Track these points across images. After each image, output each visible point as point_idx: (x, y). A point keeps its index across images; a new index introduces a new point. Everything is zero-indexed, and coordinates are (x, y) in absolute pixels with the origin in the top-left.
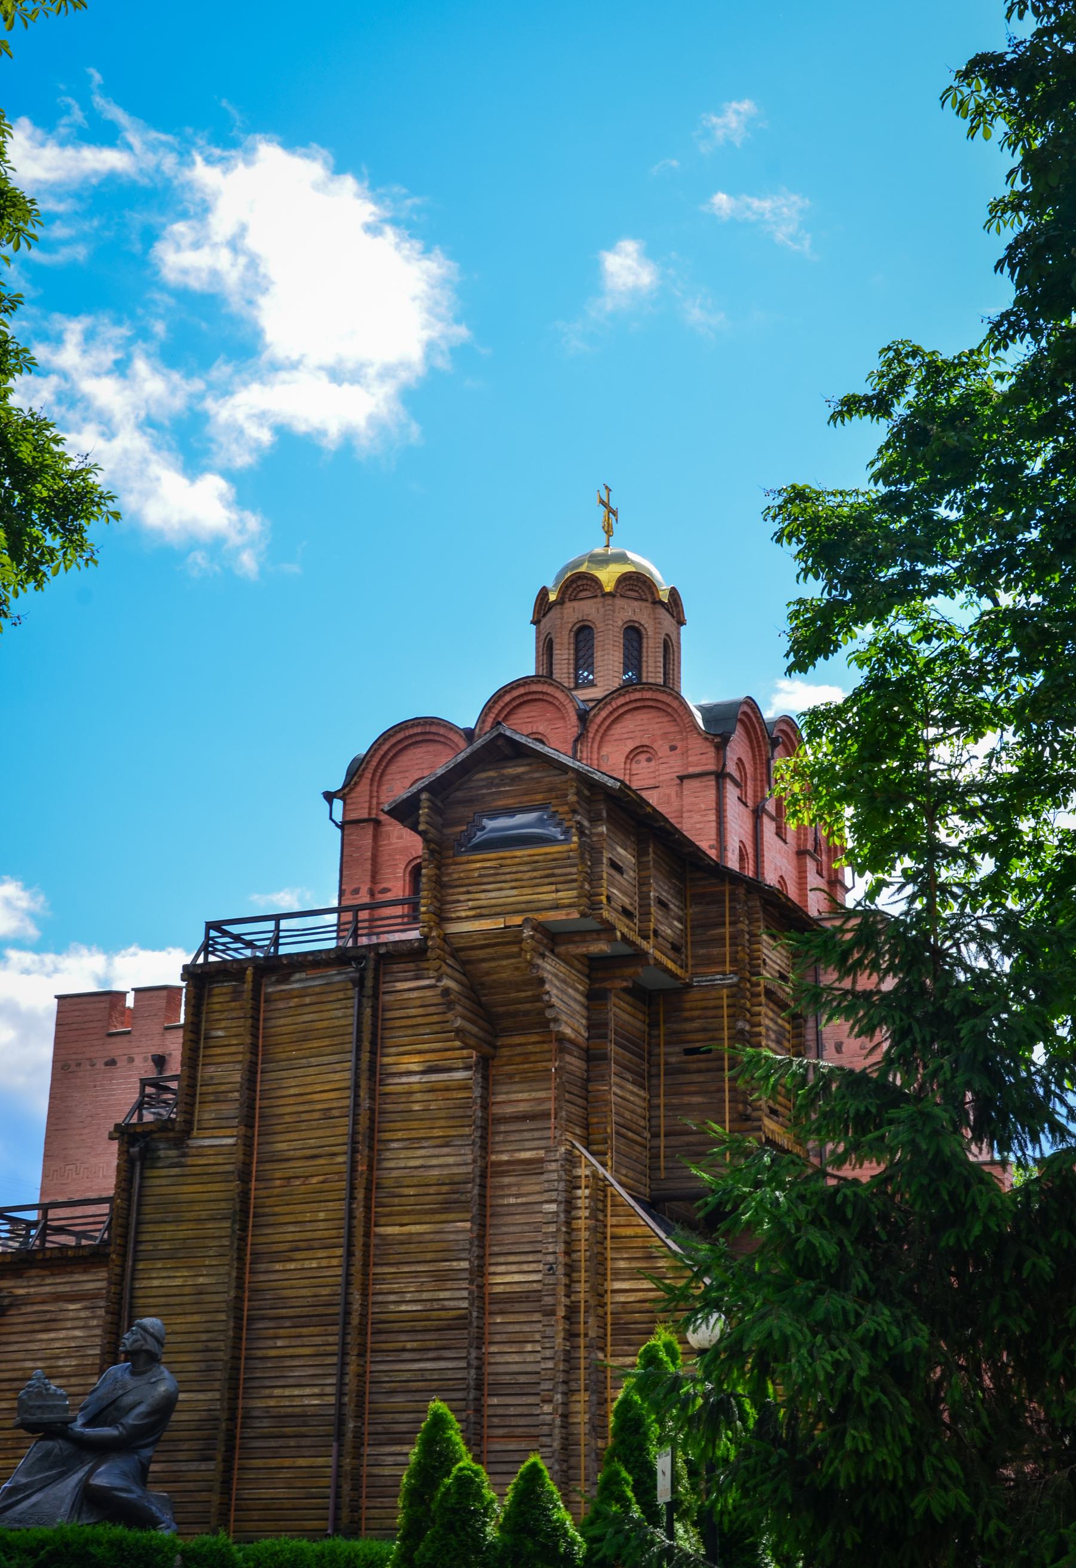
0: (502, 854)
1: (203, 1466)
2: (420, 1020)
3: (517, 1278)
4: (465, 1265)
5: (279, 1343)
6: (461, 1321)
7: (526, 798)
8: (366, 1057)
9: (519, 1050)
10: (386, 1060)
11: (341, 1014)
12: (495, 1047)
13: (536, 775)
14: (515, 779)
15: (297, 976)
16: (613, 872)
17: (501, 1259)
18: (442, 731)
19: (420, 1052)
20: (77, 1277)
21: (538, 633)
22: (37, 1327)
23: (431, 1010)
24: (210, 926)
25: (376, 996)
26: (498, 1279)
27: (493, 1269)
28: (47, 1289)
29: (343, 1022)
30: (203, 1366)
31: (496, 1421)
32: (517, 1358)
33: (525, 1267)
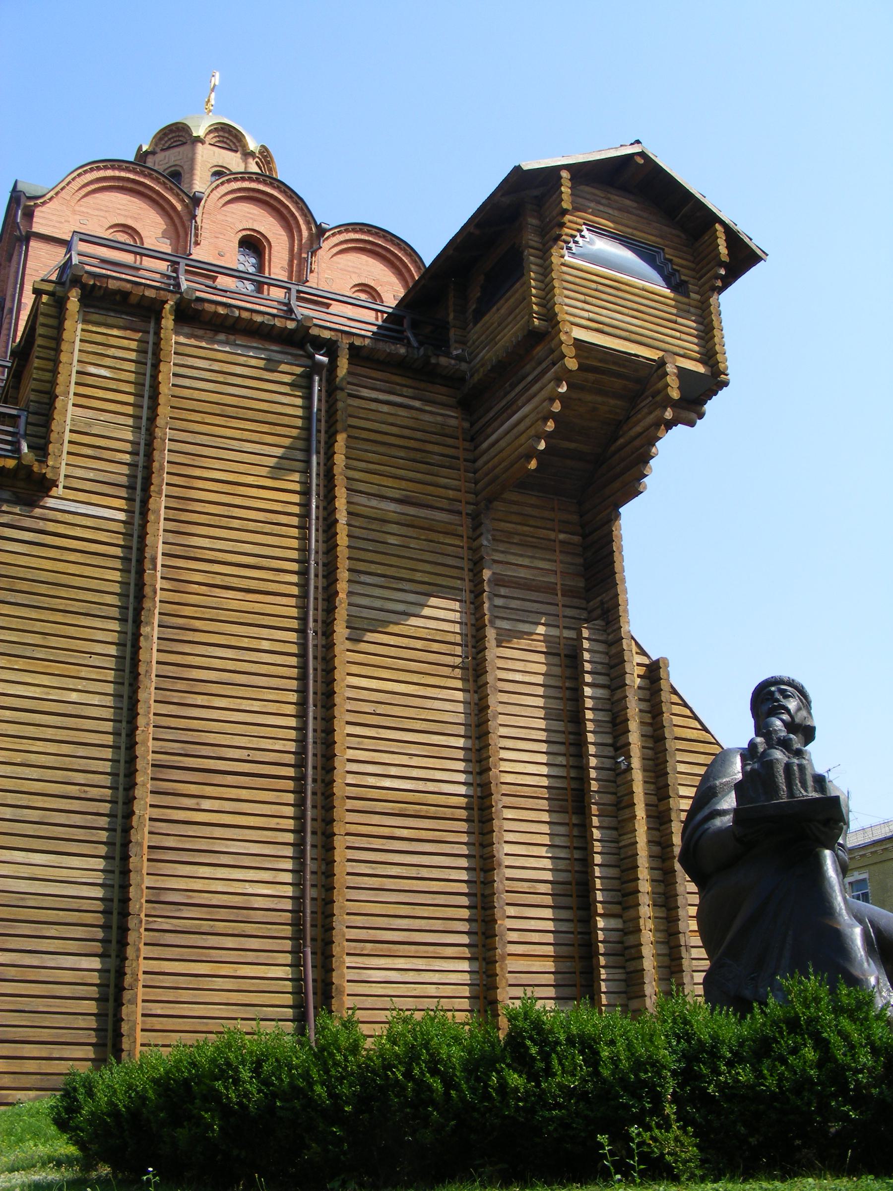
5: (206, 804)
9: (515, 508)
23: (406, 432)
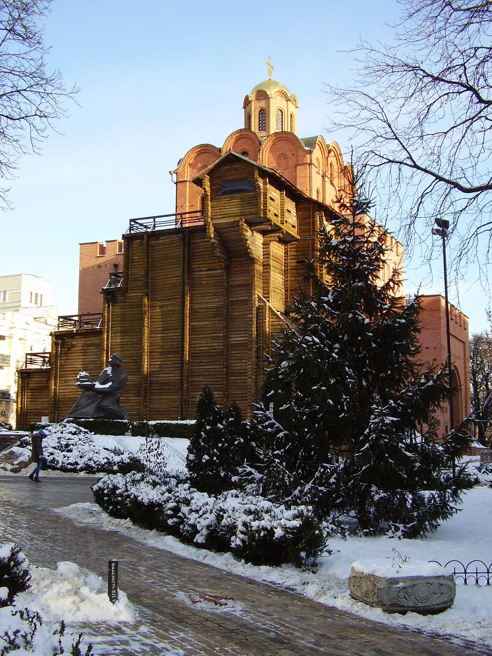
0: (232, 196)
1: (137, 398)
2: (205, 253)
3: (239, 339)
4: (222, 334)
6: (221, 353)
7: (239, 176)
8: (186, 265)
10: (194, 266)
11: (178, 251)
12: (231, 262)
13: (243, 168)
14: (236, 169)
15: (162, 238)
16: (271, 201)
17: (234, 333)
18: (211, 149)
19: (205, 264)
20: (92, 339)
21: (245, 111)
23: (209, 249)
24: (131, 220)
25: (189, 245)
27: (231, 336)
29: (178, 254)
31: (233, 384)
32: (240, 365)
33: (242, 335)
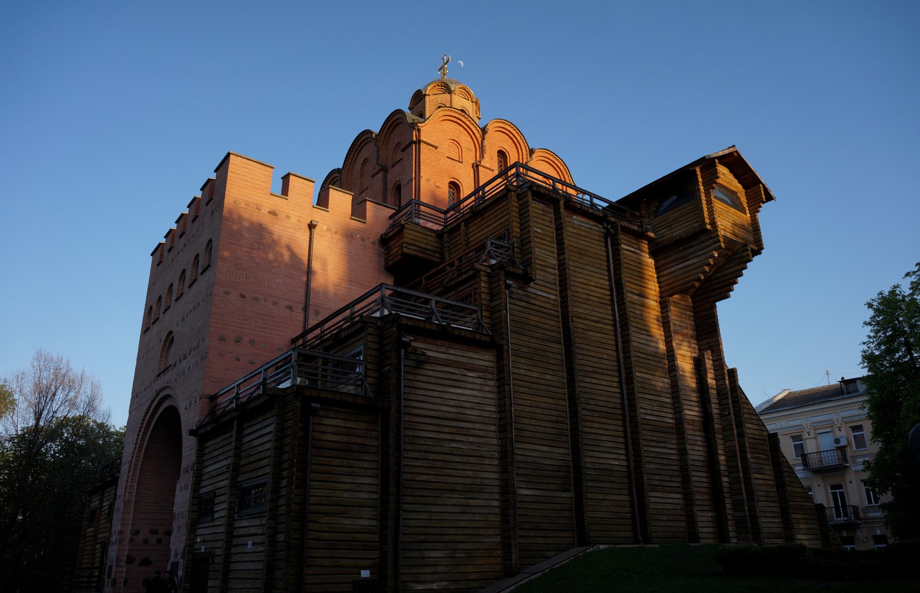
1: (564, 495)
5: (595, 425)
20: (471, 354)
22: (447, 382)
26: (695, 413)
28: (451, 357)
30: (555, 431)
